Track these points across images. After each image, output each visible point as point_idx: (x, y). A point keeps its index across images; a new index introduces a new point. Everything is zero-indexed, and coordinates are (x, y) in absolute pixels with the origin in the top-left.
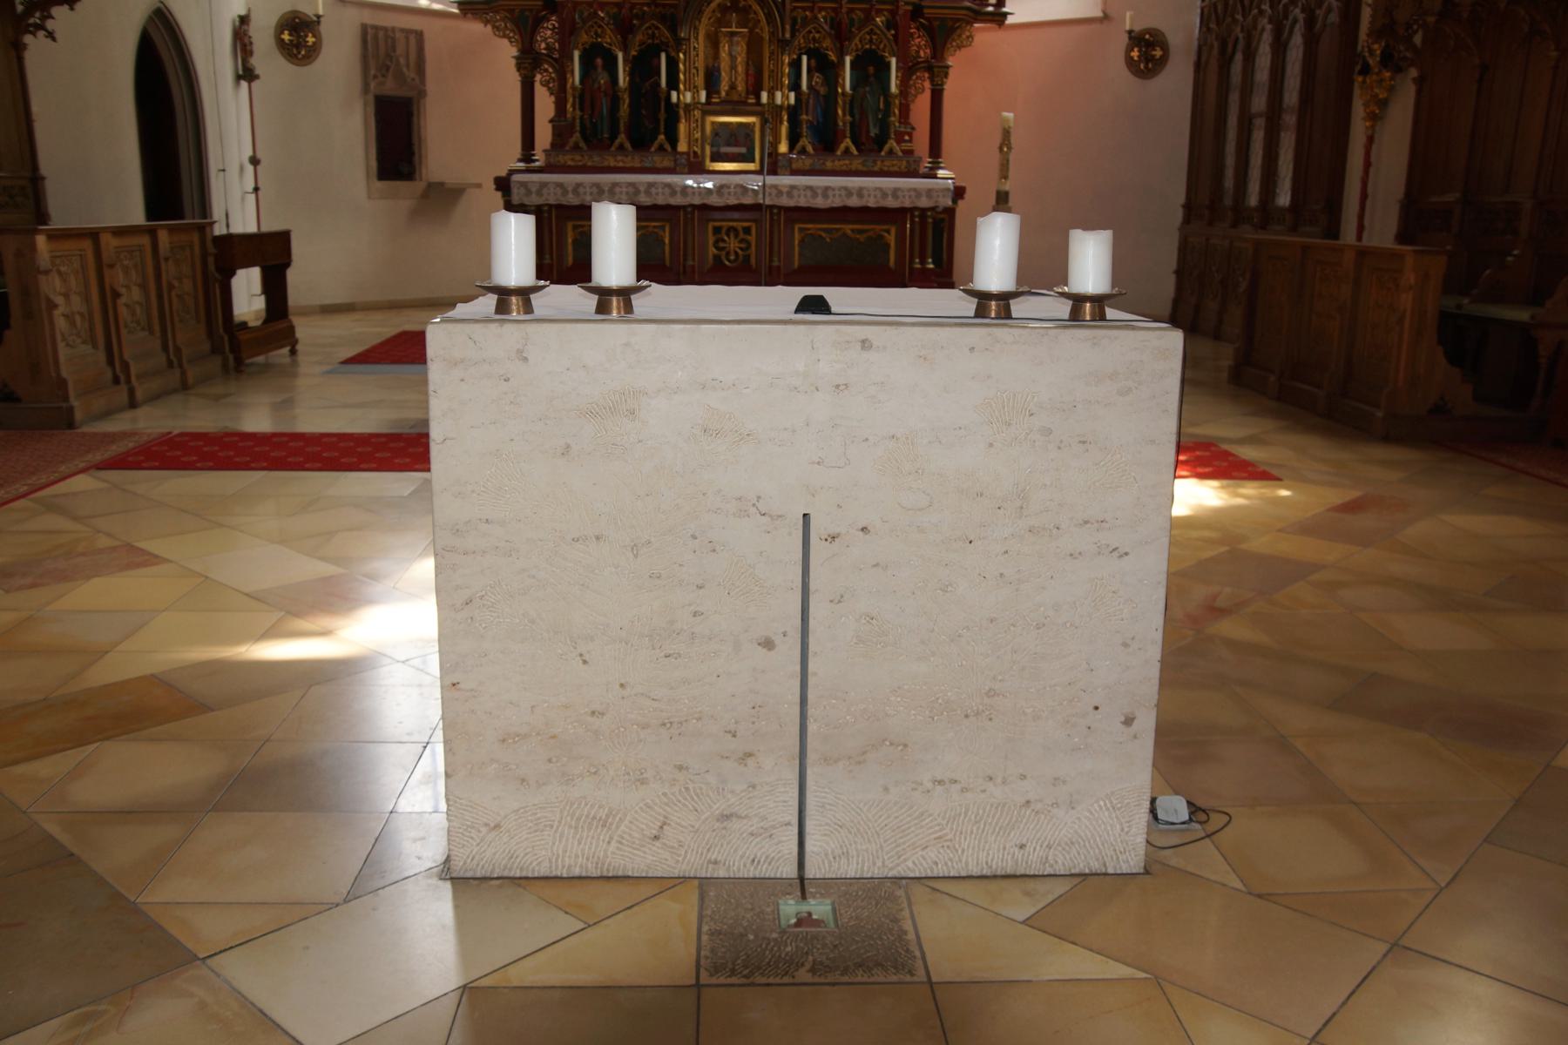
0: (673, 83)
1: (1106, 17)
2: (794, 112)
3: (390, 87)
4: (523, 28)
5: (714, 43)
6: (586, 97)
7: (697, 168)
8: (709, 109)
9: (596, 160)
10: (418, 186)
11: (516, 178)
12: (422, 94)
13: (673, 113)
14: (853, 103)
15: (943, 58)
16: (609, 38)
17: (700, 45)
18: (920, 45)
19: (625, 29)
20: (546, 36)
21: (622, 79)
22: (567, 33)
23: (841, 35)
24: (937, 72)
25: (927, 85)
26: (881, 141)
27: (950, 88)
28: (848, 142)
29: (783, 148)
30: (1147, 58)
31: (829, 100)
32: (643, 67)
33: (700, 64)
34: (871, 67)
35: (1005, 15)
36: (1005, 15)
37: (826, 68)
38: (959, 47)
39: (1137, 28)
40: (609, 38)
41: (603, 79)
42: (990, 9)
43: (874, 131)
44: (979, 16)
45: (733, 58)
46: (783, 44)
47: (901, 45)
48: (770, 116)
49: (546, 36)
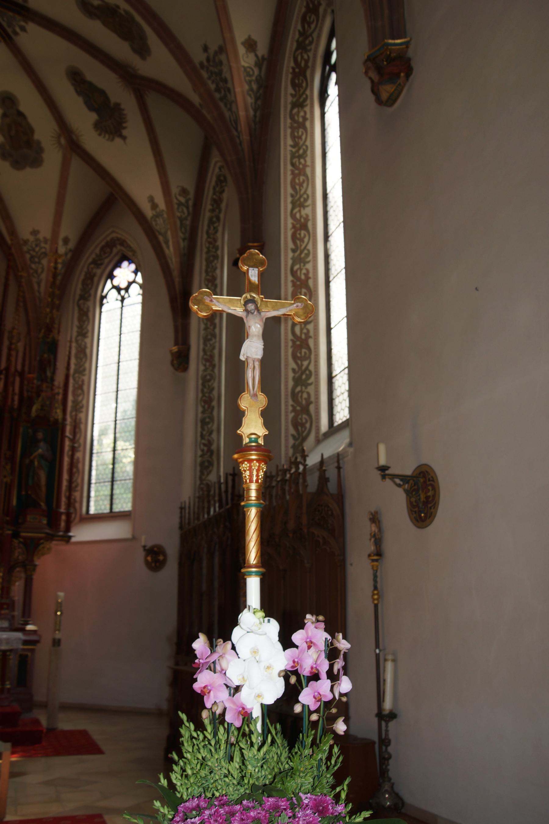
15: (32, 561)
25: (23, 575)
27: (36, 577)
30: (156, 561)
35: (70, 537)
36: (70, 537)
38: (43, 555)
39: (149, 545)
42: (61, 533)
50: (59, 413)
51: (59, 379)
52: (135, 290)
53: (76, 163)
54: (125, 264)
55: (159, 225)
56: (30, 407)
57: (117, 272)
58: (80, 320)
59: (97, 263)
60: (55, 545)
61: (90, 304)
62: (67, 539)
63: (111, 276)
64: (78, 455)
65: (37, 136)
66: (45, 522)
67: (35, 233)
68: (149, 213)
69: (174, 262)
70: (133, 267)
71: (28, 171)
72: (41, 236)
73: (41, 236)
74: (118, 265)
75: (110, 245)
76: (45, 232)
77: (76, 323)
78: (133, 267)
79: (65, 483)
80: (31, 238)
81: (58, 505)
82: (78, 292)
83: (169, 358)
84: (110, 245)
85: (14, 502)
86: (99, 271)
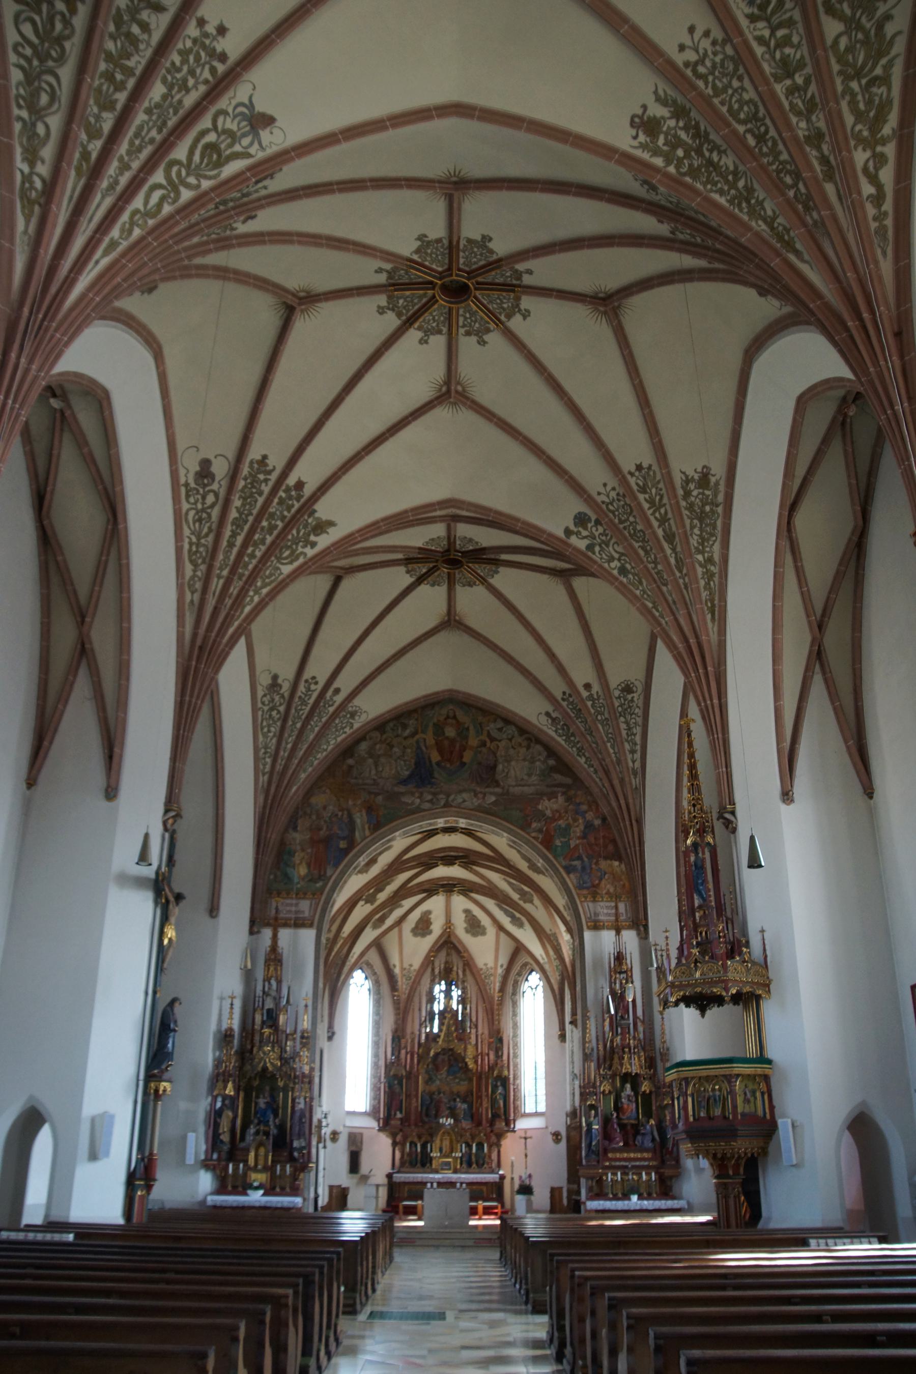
0: (431, 1151)
1: (547, 1127)
2: (461, 1158)
3: (354, 1148)
4: (393, 1135)
5: (441, 1140)
6: (410, 1154)
7: (437, 1172)
8: (440, 1157)
9: (412, 1170)
10: (358, 1176)
11: (395, 1175)
12: (361, 1150)
13: (431, 1159)
14: (476, 1154)
16: (416, 1140)
17: (438, 1142)
18: (493, 1139)
19: (420, 1137)
20: (399, 1138)
21: (419, 1150)
22: (405, 1138)
23: (473, 1139)
24: (499, 1145)
26: (483, 1164)
27: (502, 1150)
28: (474, 1165)
29: (458, 1167)
31: (470, 1154)
32: (424, 1146)
33: (438, 1146)
34: (480, 1146)
37: (469, 1146)
40: (416, 1140)
41: (414, 1149)
43: (481, 1162)
44: (508, 1131)
45: (446, 1143)
46: (458, 1142)
47: (488, 1139)
48: (455, 1158)
49: (399, 1138)
50: (506, 1073)
51: (505, 1057)
52: (540, 989)
53: (502, 935)
54: (534, 973)
55: (547, 967)
56: (493, 1071)
57: (530, 978)
58: (513, 1007)
59: (519, 974)
60: (509, 1134)
61: (517, 997)
62: (515, 1131)
63: (527, 980)
64: (518, 1082)
65: (482, 923)
66: (504, 1124)
67: (486, 965)
68: (541, 961)
69: (556, 987)
70: (538, 976)
71: (480, 938)
72: (489, 966)
73: (489, 966)
74: (530, 973)
75: (526, 964)
76: (491, 964)
77: (511, 1009)
78: (538, 976)
79: (512, 1098)
80: (484, 967)
81: (509, 1115)
82: (511, 991)
83: (557, 1037)
84: (526, 964)
85: (490, 1115)
86: (520, 979)
